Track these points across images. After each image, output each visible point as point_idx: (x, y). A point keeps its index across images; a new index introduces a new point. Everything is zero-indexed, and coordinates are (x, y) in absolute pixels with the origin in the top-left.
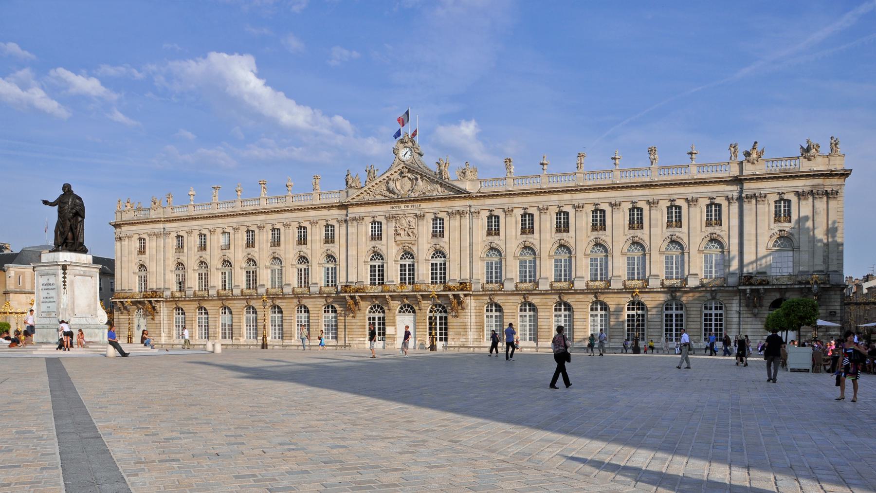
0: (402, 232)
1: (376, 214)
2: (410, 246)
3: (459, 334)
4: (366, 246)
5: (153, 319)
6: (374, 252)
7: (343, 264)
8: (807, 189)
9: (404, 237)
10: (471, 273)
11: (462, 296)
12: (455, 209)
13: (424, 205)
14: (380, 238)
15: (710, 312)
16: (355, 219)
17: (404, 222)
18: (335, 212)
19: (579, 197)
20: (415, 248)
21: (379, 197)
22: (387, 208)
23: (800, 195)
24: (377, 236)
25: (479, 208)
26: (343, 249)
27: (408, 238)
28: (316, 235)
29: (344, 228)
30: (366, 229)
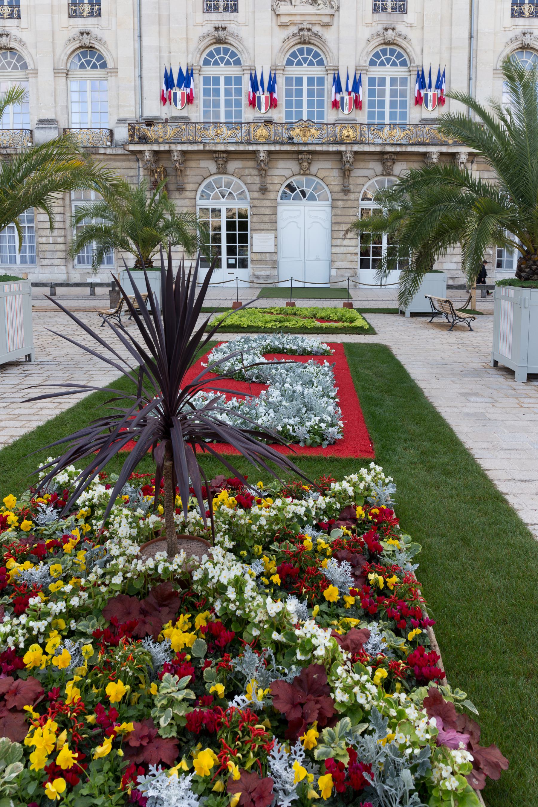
2: (316, 29)
7: (127, 72)
20: (329, 35)
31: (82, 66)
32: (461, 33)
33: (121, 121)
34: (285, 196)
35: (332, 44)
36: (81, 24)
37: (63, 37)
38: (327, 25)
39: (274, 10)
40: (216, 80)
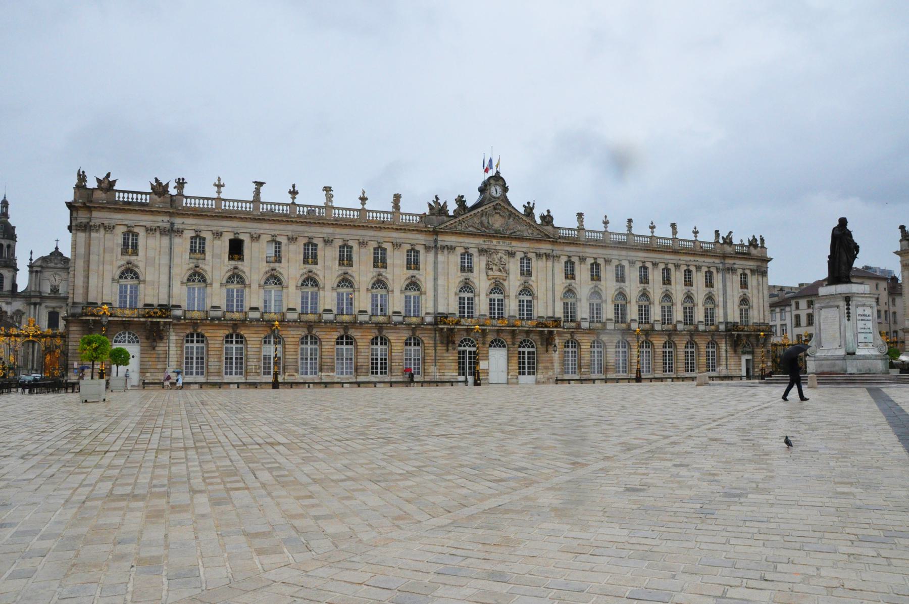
0: (494, 267)
1: (468, 245)
3: (546, 368)
4: (457, 278)
5: (154, 349)
6: (466, 283)
7: (430, 293)
10: (554, 312)
12: (543, 251)
13: (514, 243)
14: (470, 270)
16: (443, 248)
17: (496, 257)
18: (420, 239)
20: (506, 284)
21: (471, 229)
22: (479, 241)
24: (467, 268)
25: (560, 253)
26: (431, 277)
27: (499, 274)
28: (397, 260)
30: (455, 259)
32: (550, 284)
33: (427, 314)
34: (490, 346)
36: (412, 272)
37: (405, 277)
38: (505, 280)
40: (464, 299)
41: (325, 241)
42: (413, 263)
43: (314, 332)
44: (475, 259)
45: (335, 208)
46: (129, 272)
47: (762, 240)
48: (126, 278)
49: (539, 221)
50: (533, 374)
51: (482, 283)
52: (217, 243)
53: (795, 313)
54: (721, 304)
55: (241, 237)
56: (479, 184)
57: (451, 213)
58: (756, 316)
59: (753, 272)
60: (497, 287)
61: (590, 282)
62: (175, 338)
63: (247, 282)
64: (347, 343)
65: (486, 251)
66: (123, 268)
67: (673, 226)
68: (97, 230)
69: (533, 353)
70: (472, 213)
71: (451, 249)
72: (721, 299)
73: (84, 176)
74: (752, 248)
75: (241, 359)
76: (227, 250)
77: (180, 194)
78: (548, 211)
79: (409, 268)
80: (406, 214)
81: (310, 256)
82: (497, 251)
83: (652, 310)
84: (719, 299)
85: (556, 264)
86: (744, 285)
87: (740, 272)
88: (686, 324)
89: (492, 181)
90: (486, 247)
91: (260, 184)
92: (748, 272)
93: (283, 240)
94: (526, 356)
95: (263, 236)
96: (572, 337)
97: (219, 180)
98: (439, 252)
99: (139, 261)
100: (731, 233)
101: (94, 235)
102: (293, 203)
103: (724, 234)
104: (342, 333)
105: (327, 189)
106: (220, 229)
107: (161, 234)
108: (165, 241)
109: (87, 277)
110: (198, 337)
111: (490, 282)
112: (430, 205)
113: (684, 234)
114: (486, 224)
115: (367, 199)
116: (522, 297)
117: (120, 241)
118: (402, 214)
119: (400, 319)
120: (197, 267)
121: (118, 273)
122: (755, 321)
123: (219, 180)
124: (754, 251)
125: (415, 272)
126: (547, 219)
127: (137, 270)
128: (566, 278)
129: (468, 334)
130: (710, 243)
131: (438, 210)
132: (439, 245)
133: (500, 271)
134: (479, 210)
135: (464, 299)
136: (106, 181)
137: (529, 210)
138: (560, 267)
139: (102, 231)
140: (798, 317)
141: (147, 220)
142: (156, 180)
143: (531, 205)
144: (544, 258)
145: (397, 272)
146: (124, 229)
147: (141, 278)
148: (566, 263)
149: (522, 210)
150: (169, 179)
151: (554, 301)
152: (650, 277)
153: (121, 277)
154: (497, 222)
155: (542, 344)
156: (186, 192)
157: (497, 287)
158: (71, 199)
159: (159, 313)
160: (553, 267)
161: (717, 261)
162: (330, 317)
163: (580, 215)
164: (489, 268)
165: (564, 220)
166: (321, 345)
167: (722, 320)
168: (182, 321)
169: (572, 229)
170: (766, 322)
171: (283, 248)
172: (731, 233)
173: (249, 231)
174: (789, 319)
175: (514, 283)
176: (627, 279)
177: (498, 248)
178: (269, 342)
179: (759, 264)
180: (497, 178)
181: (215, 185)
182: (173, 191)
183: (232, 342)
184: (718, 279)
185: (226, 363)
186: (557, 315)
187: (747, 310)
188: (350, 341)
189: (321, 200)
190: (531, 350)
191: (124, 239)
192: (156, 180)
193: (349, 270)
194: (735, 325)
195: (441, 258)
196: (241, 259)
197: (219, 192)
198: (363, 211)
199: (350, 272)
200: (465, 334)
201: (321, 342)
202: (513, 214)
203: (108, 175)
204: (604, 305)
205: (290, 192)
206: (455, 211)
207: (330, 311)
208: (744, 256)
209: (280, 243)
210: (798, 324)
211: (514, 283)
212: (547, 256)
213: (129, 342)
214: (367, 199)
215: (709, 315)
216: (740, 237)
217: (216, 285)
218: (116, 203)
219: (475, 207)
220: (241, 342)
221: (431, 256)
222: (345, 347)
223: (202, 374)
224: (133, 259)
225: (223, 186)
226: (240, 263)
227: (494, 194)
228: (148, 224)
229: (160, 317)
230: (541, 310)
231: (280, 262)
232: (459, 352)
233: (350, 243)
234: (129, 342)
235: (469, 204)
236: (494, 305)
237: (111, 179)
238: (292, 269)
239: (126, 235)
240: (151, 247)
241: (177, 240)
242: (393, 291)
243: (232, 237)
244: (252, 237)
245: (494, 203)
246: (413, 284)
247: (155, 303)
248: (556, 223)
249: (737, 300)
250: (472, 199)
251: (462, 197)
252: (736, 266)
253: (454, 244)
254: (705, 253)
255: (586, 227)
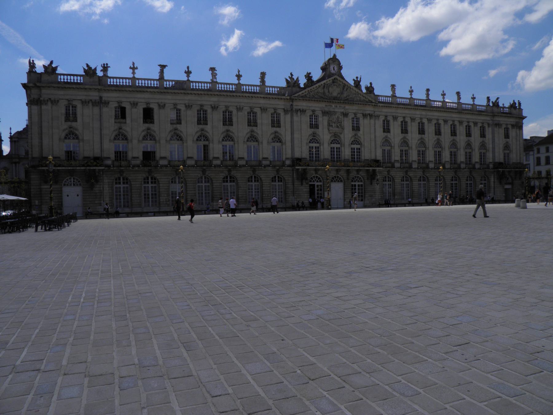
0: (333, 125)
2: (339, 134)
4: (307, 132)
7: (289, 144)
8: (514, 123)
9: (334, 129)
10: (376, 156)
11: (377, 171)
12: (367, 112)
13: (347, 107)
14: (317, 126)
15: (231, 184)
16: (297, 111)
18: (280, 104)
19: (430, 114)
20: (342, 136)
21: (316, 96)
22: (323, 105)
23: (513, 126)
24: (314, 126)
27: (337, 129)
28: (264, 120)
29: (288, 117)
30: (306, 119)
31: (274, 142)
32: (373, 137)
33: (287, 159)
34: (332, 181)
35: (343, 139)
36: (275, 129)
38: (341, 133)
39: (328, 129)
41: (212, 107)
42: (276, 123)
43: (207, 174)
44: (320, 119)
45: (219, 83)
46: (71, 134)
47: (520, 104)
48: (69, 138)
49: (364, 91)
50: (362, 200)
51: (325, 135)
52: (134, 110)
53: (536, 156)
54: (491, 149)
55: (151, 106)
56: (321, 64)
57: (302, 86)
58: (514, 158)
59: (513, 126)
60: (336, 139)
61: (400, 134)
62: (107, 181)
63: (157, 139)
64: (231, 181)
65: (327, 113)
66: (67, 131)
67: (458, 93)
68: (46, 104)
69: (362, 185)
70: (317, 85)
71: (303, 111)
72: (491, 146)
73: (34, 64)
74: (512, 109)
75: (155, 194)
76: (142, 116)
77: (105, 76)
78: (371, 84)
79: (273, 126)
80: (270, 87)
81: (202, 119)
82: (335, 113)
83: (444, 154)
84: (490, 146)
85: (377, 121)
86: (507, 136)
87: (504, 126)
88: (466, 164)
89: (331, 62)
90: (326, 109)
91: (163, 67)
92: (510, 127)
93: (182, 108)
94: (357, 187)
95: (167, 105)
96: (388, 174)
97: (133, 64)
98: (294, 114)
99: (78, 125)
100: (498, 98)
101: (44, 107)
102: (188, 80)
103: (493, 99)
104: (227, 173)
105: (213, 69)
106: (136, 100)
107: (93, 105)
108: (96, 110)
109: (41, 138)
110: (123, 179)
111: (330, 135)
112: (287, 80)
113: (466, 99)
114: (327, 94)
115: (241, 76)
116: (353, 146)
117: (63, 111)
118: (267, 87)
119: (268, 163)
120: (120, 128)
121: (63, 135)
122: (514, 161)
123: (133, 64)
124: (514, 111)
125: (278, 129)
126: (370, 89)
127: (77, 132)
128: (384, 132)
129: (316, 173)
130: (483, 106)
131: (292, 83)
132: (294, 109)
133: (338, 127)
134: (322, 82)
135: (313, 147)
136: (51, 67)
137: (357, 83)
138: (379, 124)
139: (49, 103)
140: (539, 159)
141: (81, 95)
142: (87, 65)
143: (359, 79)
144: (369, 117)
145: (264, 128)
146: (66, 103)
147: (80, 137)
148: (384, 121)
149: (352, 83)
150: (96, 64)
151: (376, 148)
152: (442, 131)
153: (65, 138)
154: (335, 91)
155: (368, 179)
156: (110, 73)
157: (336, 139)
158: (25, 81)
159: (95, 163)
160: (375, 124)
161: (488, 118)
162: (218, 162)
163: (393, 86)
164: (329, 125)
165: (382, 90)
166: (212, 183)
167: (491, 161)
168: (112, 168)
169: (387, 97)
170: (521, 162)
171: (182, 113)
172: (498, 98)
173: (157, 101)
174: (532, 161)
175: (347, 135)
176: (426, 133)
177: (336, 110)
178: (175, 182)
179: (517, 120)
180: (334, 60)
181: (130, 68)
182: (100, 73)
183: (148, 183)
184: (489, 132)
185: (145, 198)
186: (378, 158)
187: (508, 154)
188: (233, 179)
189: (208, 77)
190: (360, 183)
191: (66, 109)
192: (87, 65)
193: (230, 128)
194: (500, 163)
195: (296, 118)
196: (152, 122)
197: (134, 73)
198: (239, 85)
199: (231, 130)
200: (314, 172)
201: (212, 181)
202: (345, 85)
203: (52, 62)
204: (410, 151)
205: (185, 72)
206: (305, 84)
207: (217, 158)
208: (509, 115)
209: (180, 110)
210: (538, 163)
211: (347, 135)
212: (371, 116)
213: (74, 185)
214: (241, 76)
215: (482, 156)
216: (505, 102)
217: (135, 142)
218: (60, 83)
219: (319, 81)
220: (155, 183)
221: (288, 117)
222: (229, 184)
223: (128, 207)
224: (74, 124)
225: (137, 68)
226: (151, 125)
227: (333, 71)
228: (83, 98)
229: (96, 166)
230: (366, 155)
231: (181, 124)
232: (311, 185)
233: (231, 109)
234: (74, 185)
235: (315, 79)
236: (334, 151)
237: (54, 66)
238: (190, 128)
239: (67, 108)
240: (85, 114)
241: (105, 110)
242: (262, 143)
243: (145, 106)
244: (159, 105)
245: (333, 78)
246: (277, 138)
247: (91, 155)
248: (376, 92)
249: (501, 146)
250: (317, 75)
251: (310, 73)
252: (501, 122)
253: (304, 108)
254: (480, 112)
255: (398, 95)
